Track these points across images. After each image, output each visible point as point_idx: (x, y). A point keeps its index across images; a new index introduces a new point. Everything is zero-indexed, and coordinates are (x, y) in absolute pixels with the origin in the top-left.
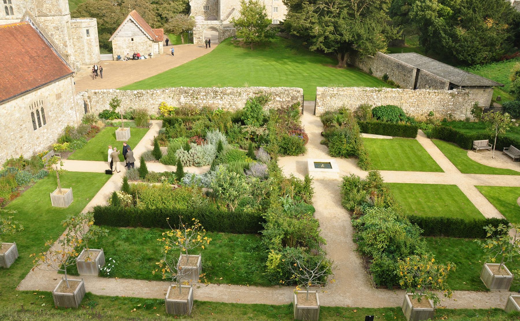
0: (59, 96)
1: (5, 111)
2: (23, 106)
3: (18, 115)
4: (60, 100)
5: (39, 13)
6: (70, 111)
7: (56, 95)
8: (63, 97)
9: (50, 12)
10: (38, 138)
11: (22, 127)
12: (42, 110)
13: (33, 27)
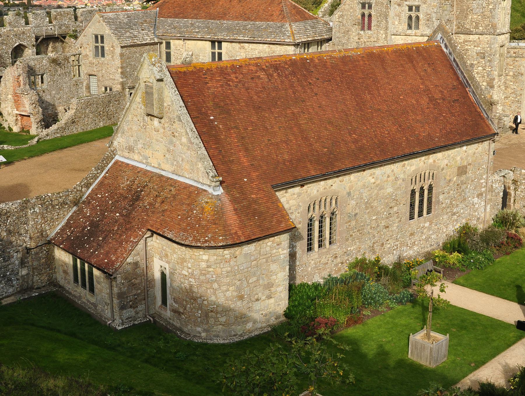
0: (462, 171)
1: (373, 181)
2: (402, 176)
3: (390, 190)
4: (463, 178)
5: (459, 28)
6: (476, 200)
7: (459, 168)
8: (470, 174)
9: (477, 27)
10: (412, 234)
12: (430, 188)
13: (445, 50)
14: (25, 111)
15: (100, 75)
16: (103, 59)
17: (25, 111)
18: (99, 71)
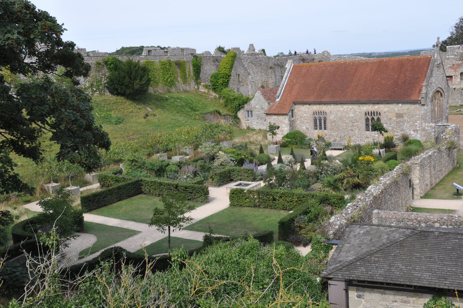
0: (399, 116)
1: (342, 109)
2: (359, 110)
3: (352, 115)
7: (397, 114)
8: (406, 118)
10: (367, 137)
11: (353, 124)
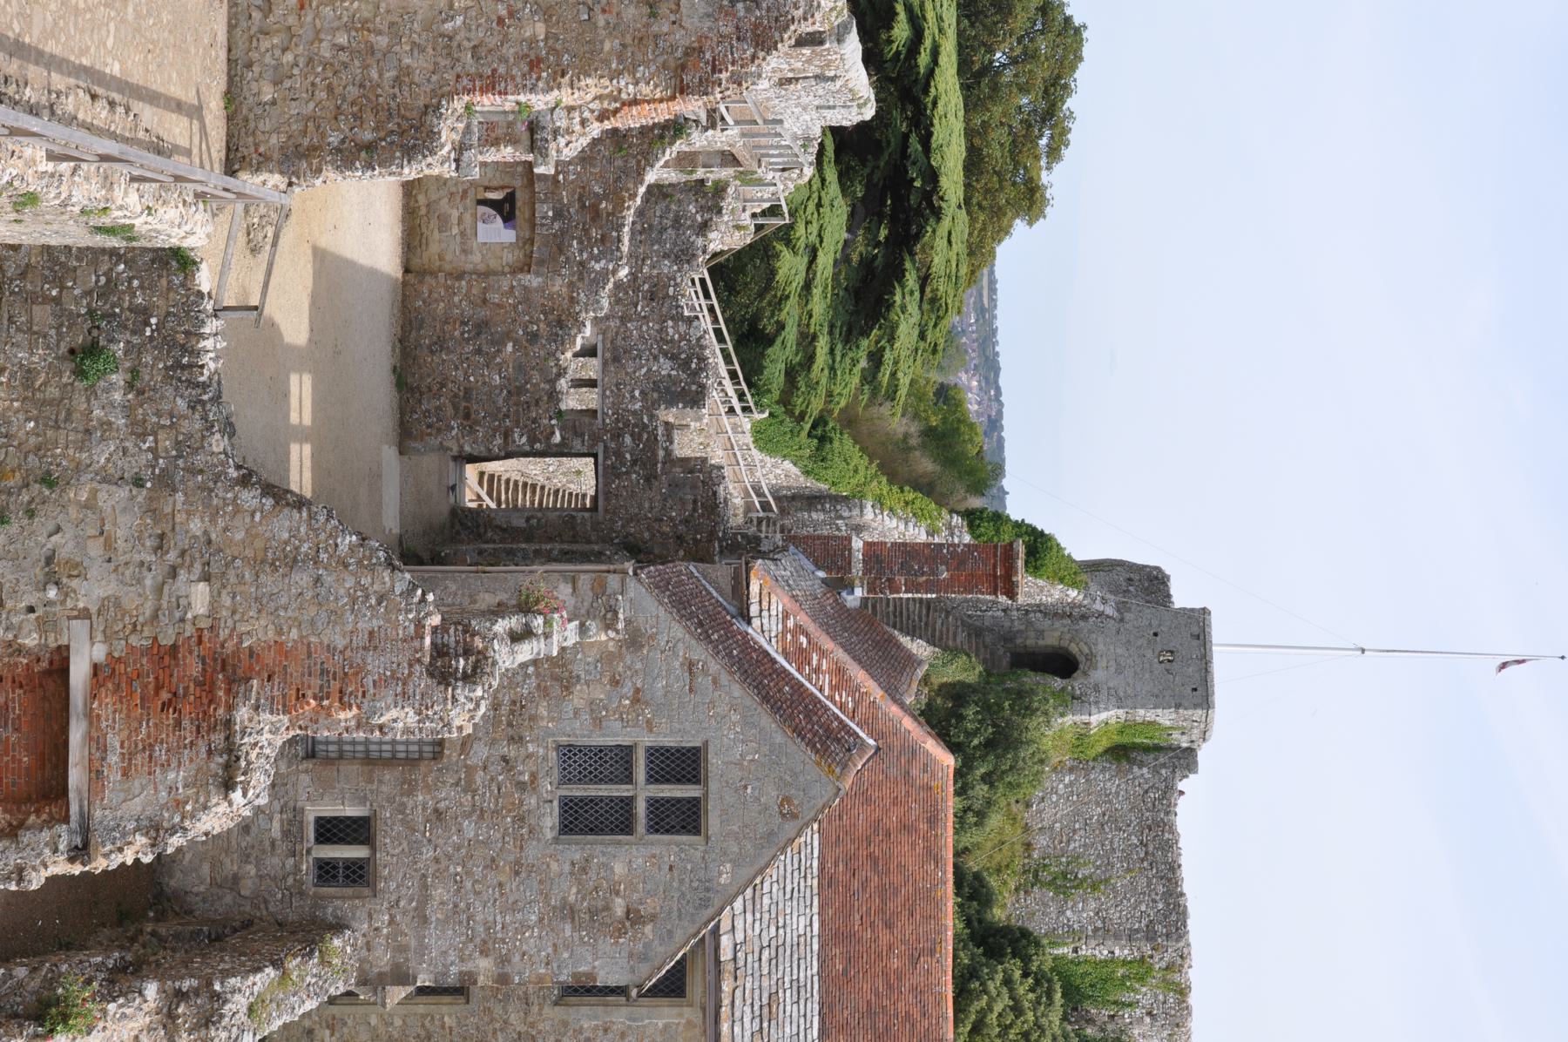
14: (96, 775)
15: (447, 796)
16: (550, 820)
17: (96, 775)
18: (470, 788)
